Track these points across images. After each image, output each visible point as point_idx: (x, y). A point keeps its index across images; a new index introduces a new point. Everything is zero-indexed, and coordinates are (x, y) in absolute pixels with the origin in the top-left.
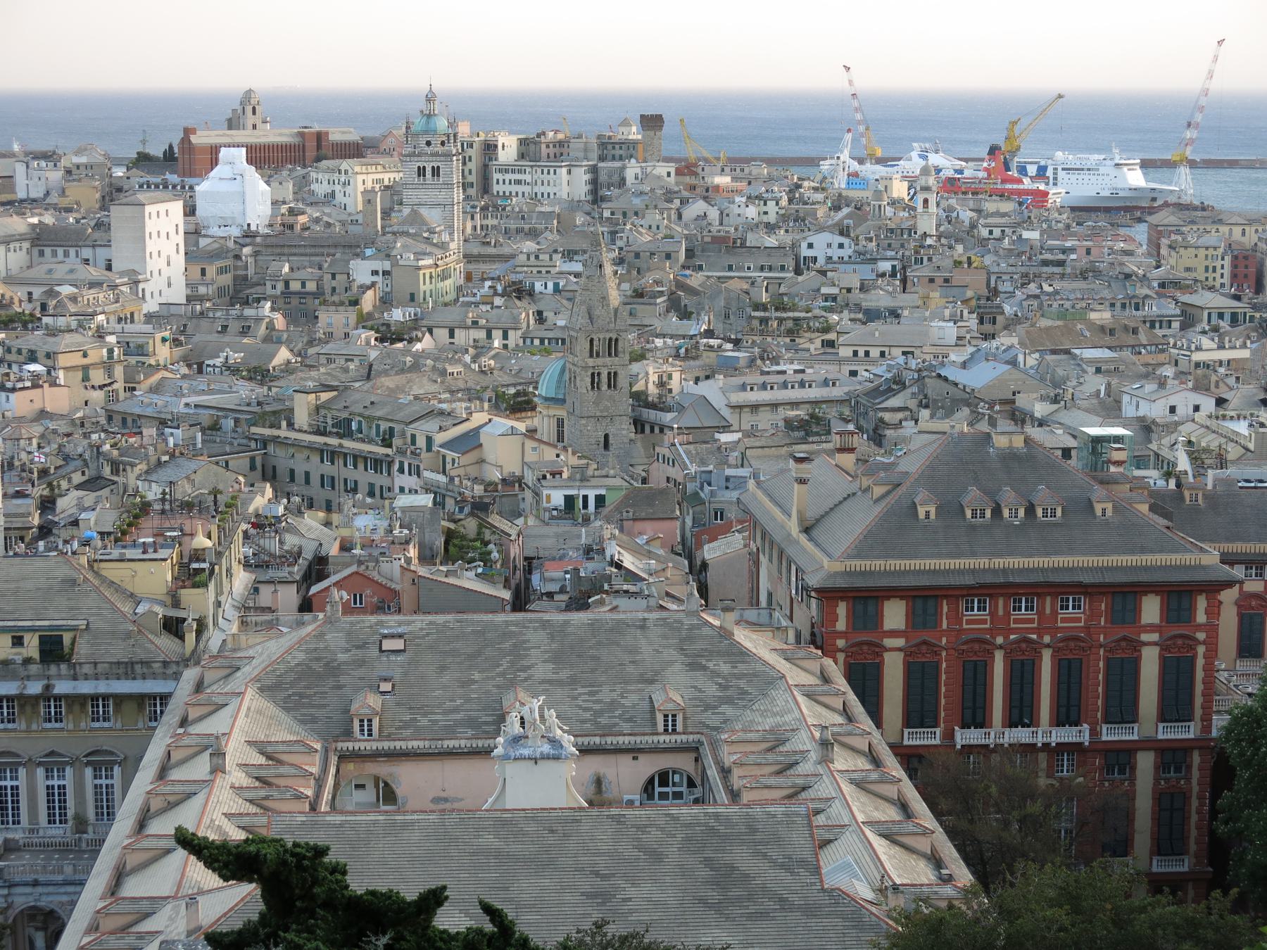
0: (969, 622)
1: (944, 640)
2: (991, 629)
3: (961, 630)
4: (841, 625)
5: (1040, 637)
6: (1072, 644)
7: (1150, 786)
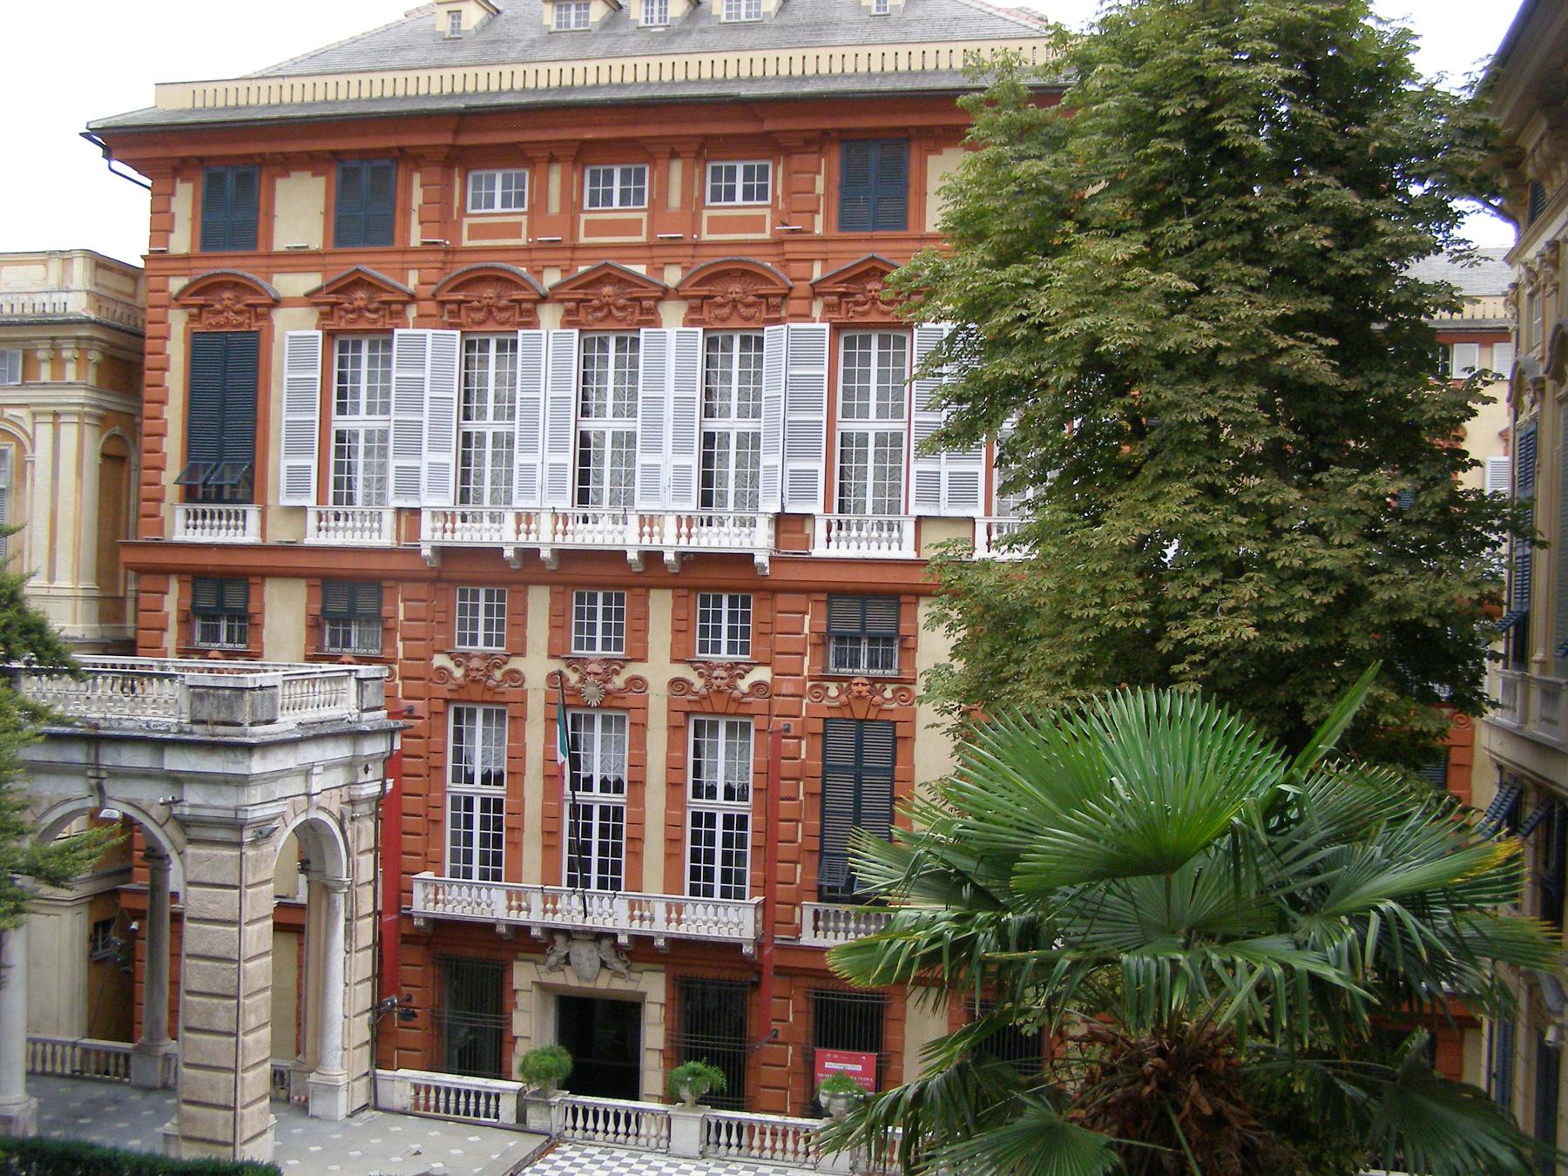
0: (475, 232)
1: (413, 280)
2: (528, 249)
4: (181, 241)
6: (735, 288)
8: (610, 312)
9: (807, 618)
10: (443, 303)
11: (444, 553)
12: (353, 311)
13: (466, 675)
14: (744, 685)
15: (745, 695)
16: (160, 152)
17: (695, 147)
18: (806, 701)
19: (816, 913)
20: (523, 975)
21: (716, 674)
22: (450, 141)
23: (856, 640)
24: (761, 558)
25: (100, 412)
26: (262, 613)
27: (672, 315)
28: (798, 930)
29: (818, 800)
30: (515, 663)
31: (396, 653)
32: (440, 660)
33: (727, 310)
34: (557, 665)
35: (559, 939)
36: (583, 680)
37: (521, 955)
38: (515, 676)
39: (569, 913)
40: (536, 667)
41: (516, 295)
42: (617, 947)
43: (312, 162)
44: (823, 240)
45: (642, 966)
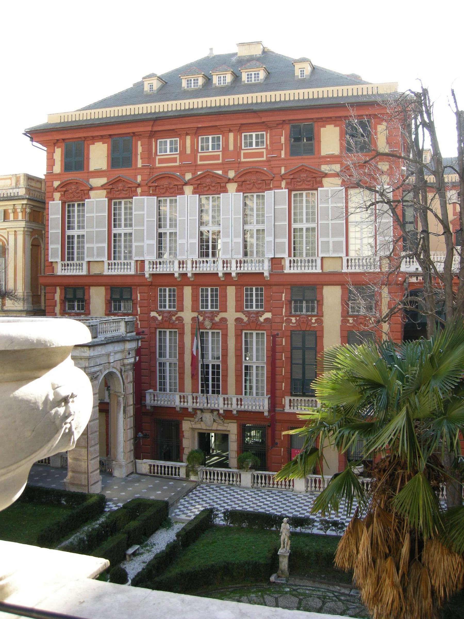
1: (139, 179)
3: (153, 168)
4: (57, 169)
5: (226, 172)
7: (340, 323)
8: (209, 188)
9: (284, 295)
10: (150, 187)
11: (153, 275)
12: (118, 191)
13: (162, 319)
14: (262, 319)
15: (262, 323)
16: (50, 138)
17: (238, 128)
18: (284, 324)
19: (290, 400)
20: (186, 425)
21: (251, 316)
22: (149, 129)
23: (301, 302)
24: (266, 274)
25: (31, 230)
26: (89, 299)
27: (232, 187)
28: (284, 406)
29: (289, 360)
30: (180, 314)
31: (137, 312)
32: (153, 314)
33: (251, 186)
34: (195, 314)
35: (199, 412)
36: (204, 319)
37: (185, 418)
38: (180, 319)
39: (202, 402)
40: (187, 315)
41: (176, 183)
42: (219, 414)
43: (102, 138)
44: (283, 160)
45: (229, 421)
